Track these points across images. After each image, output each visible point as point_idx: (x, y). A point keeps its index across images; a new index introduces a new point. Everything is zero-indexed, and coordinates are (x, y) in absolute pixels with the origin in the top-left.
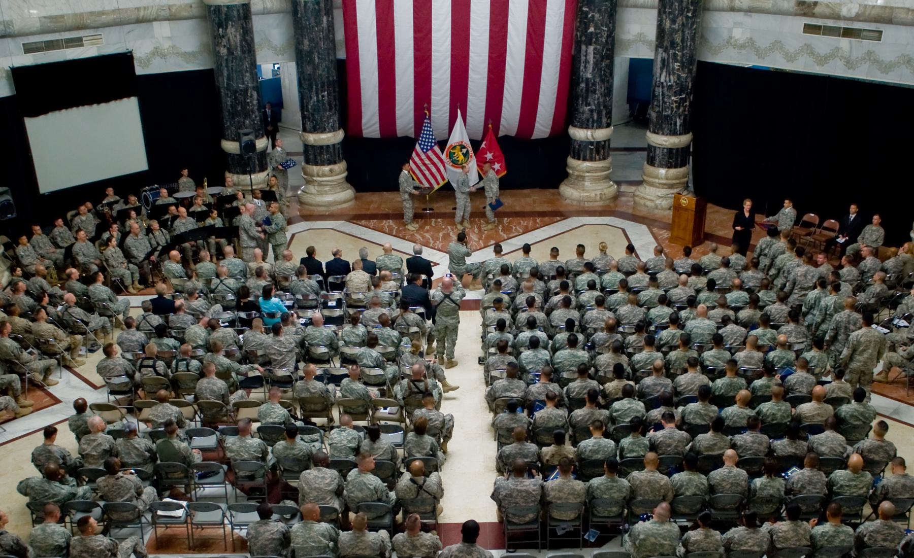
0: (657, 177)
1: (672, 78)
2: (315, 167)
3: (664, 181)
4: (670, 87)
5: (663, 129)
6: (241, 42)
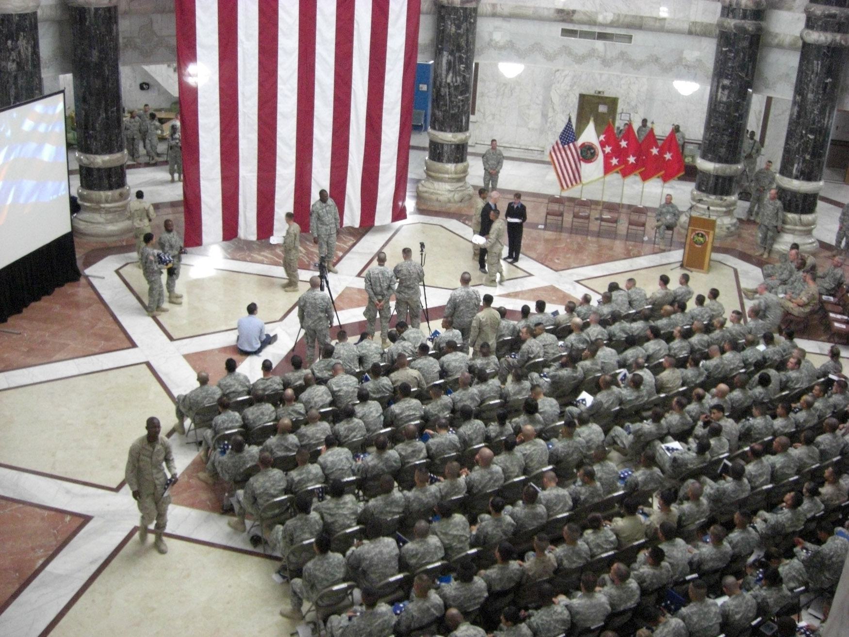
0: (447, 172)
1: (458, 79)
2: (102, 193)
3: (454, 176)
4: (456, 88)
5: (451, 127)
6: (32, 55)
